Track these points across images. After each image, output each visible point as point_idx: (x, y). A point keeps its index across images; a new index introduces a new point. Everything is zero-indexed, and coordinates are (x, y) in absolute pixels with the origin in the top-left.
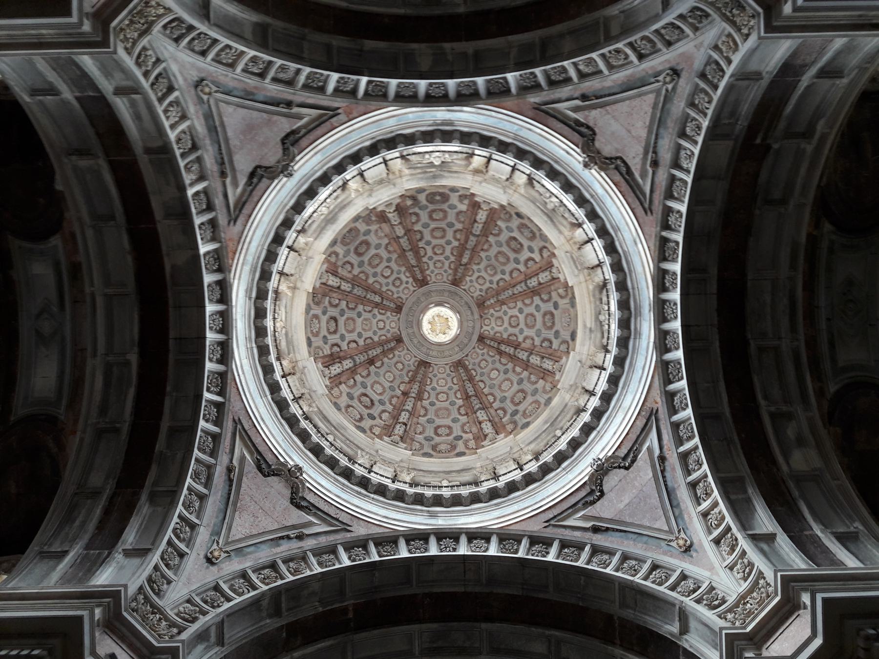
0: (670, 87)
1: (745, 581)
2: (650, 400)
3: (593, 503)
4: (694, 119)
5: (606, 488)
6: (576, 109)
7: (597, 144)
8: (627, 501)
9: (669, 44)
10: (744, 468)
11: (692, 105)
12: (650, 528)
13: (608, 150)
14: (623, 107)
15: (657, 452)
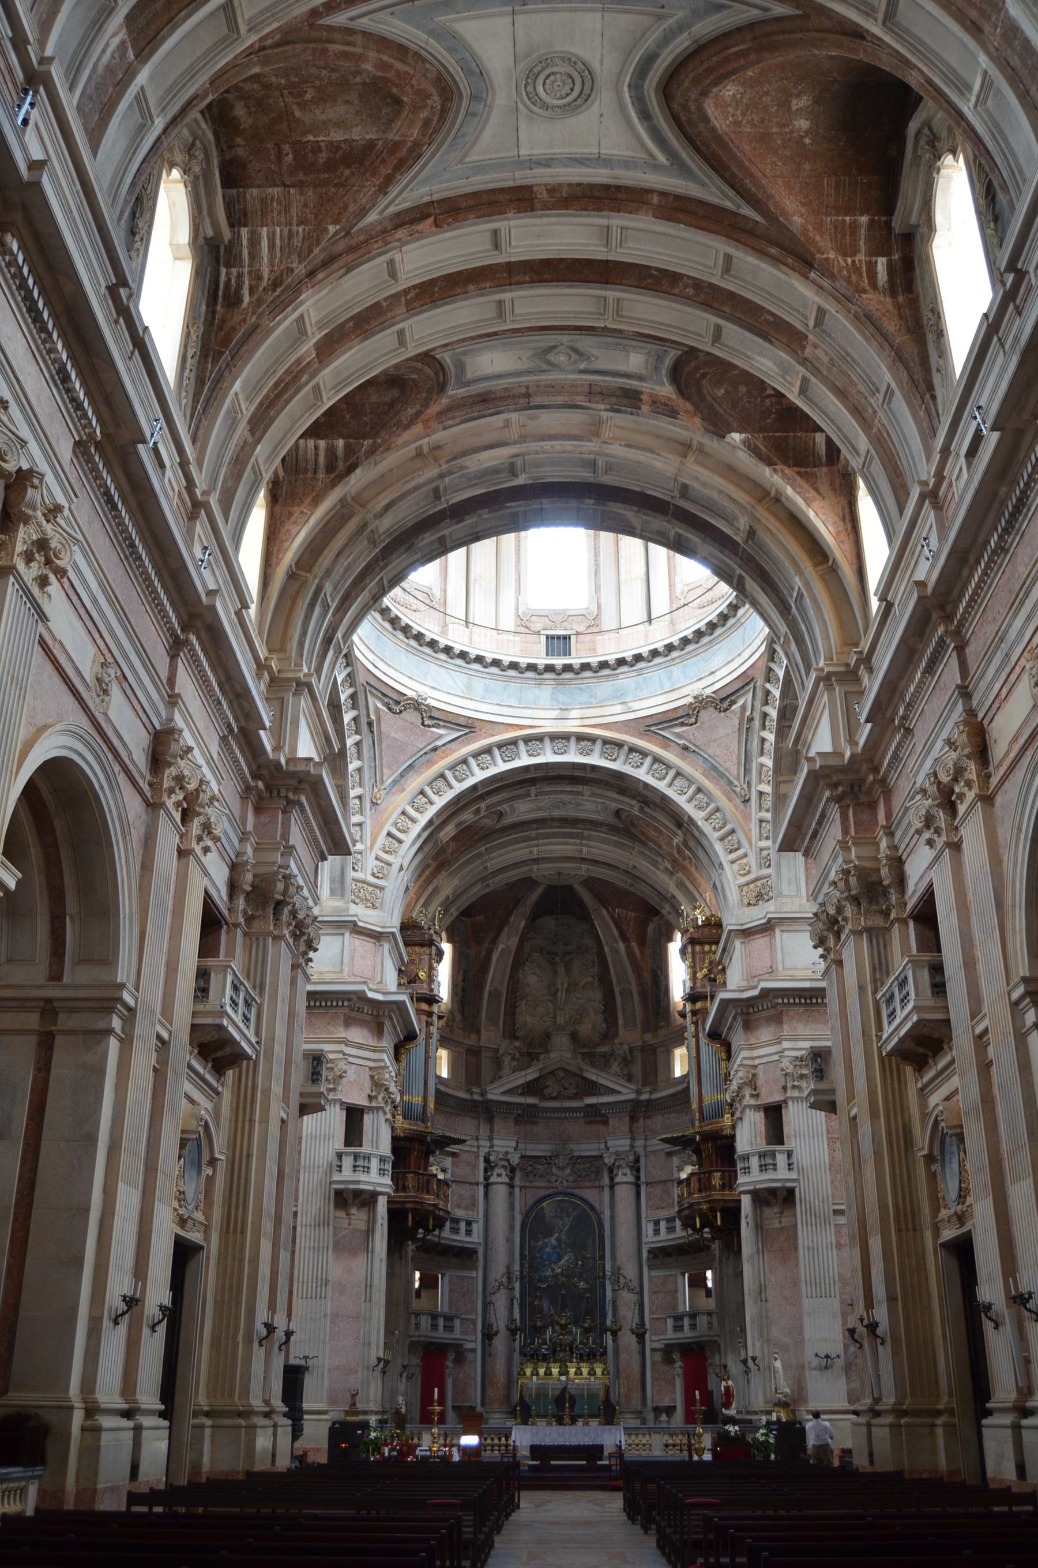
0: (738, 789)
1: (373, 875)
2: (482, 724)
3: (390, 709)
4: (708, 804)
5: (404, 714)
6: (743, 708)
7: (712, 709)
8: (397, 737)
9: (761, 821)
10: (437, 823)
11: (718, 810)
12: (382, 765)
13: (704, 715)
14: (734, 746)
15: (439, 743)
